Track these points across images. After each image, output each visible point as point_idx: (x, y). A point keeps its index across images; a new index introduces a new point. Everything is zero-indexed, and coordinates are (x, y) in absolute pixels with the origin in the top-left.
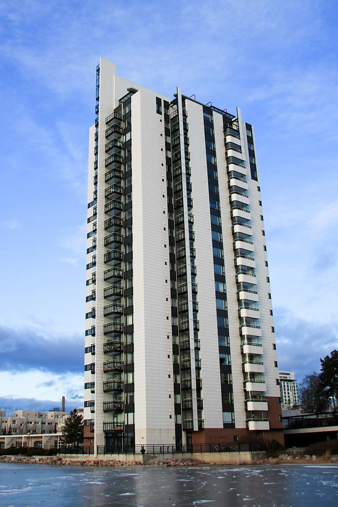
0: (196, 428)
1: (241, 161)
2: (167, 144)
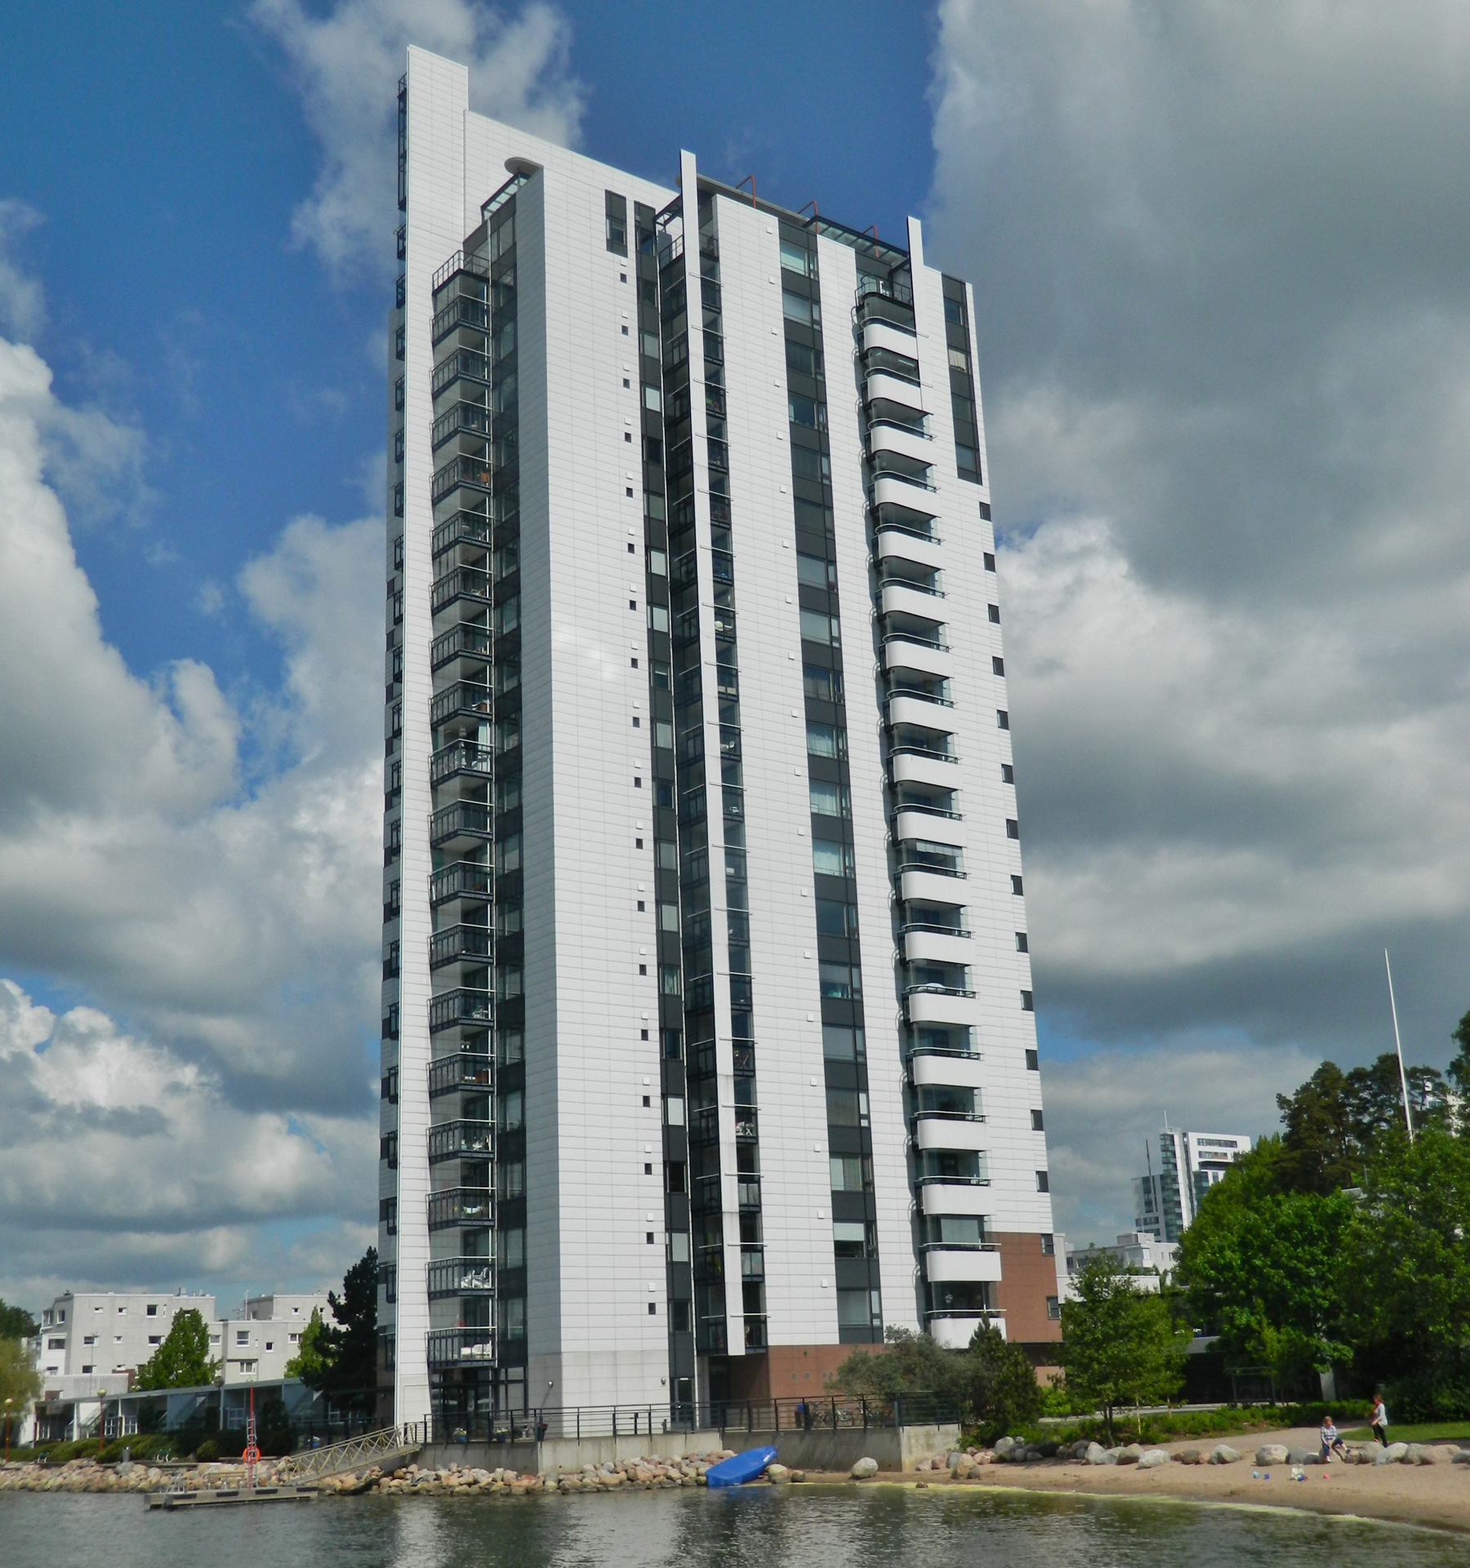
0: (736, 1345)
2: (643, 357)
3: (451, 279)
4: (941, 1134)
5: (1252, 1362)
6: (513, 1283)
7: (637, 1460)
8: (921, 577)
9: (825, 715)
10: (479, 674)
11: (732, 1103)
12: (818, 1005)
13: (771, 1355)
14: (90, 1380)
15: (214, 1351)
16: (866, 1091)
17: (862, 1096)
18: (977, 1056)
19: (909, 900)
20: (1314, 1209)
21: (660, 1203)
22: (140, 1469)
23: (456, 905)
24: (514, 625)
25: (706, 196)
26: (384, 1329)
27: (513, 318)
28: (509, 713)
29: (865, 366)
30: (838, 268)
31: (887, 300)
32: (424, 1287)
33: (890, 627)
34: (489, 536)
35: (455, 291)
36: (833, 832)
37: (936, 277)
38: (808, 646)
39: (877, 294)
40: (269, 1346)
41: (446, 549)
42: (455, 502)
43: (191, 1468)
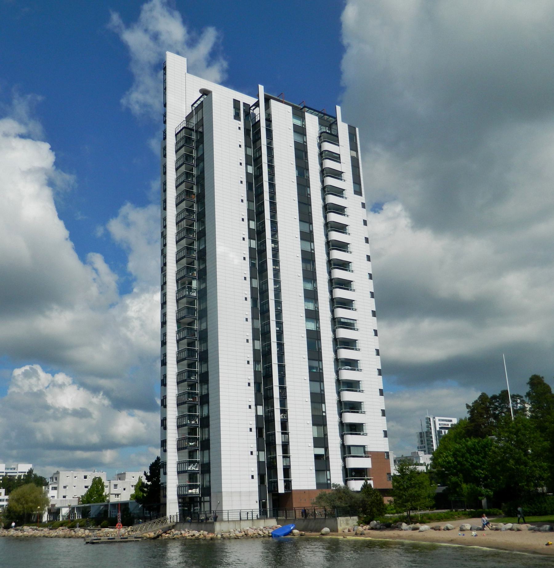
0: (281, 489)
3: (181, 130)
4: (350, 418)
6: (206, 468)
7: (248, 528)
9: (310, 275)
10: (192, 263)
11: (279, 407)
12: (308, 374)
13: (293, 493)
14: (66, 500)
15: (106, 491)
16: (325, 403)
17: (323, 405)
18: (362, 391)
21: (255, 441)
22: (82, 530)
23: (185, 341)
24: (203, 246)
25: (267, 100)
26: (162, 484)
27: (203, 143)
28: (202, 276)
29: (322, 157)
30: (312, 123)
31: (329, 134)
32: (176, 469)
34: (195, 216)
35: (183, 134)
36: (312, 315)
37: (346, 126)
38: (303, 252)
39: (326, 132)
41: (181, 221)
42: (183, 205)
43: (99, 530)
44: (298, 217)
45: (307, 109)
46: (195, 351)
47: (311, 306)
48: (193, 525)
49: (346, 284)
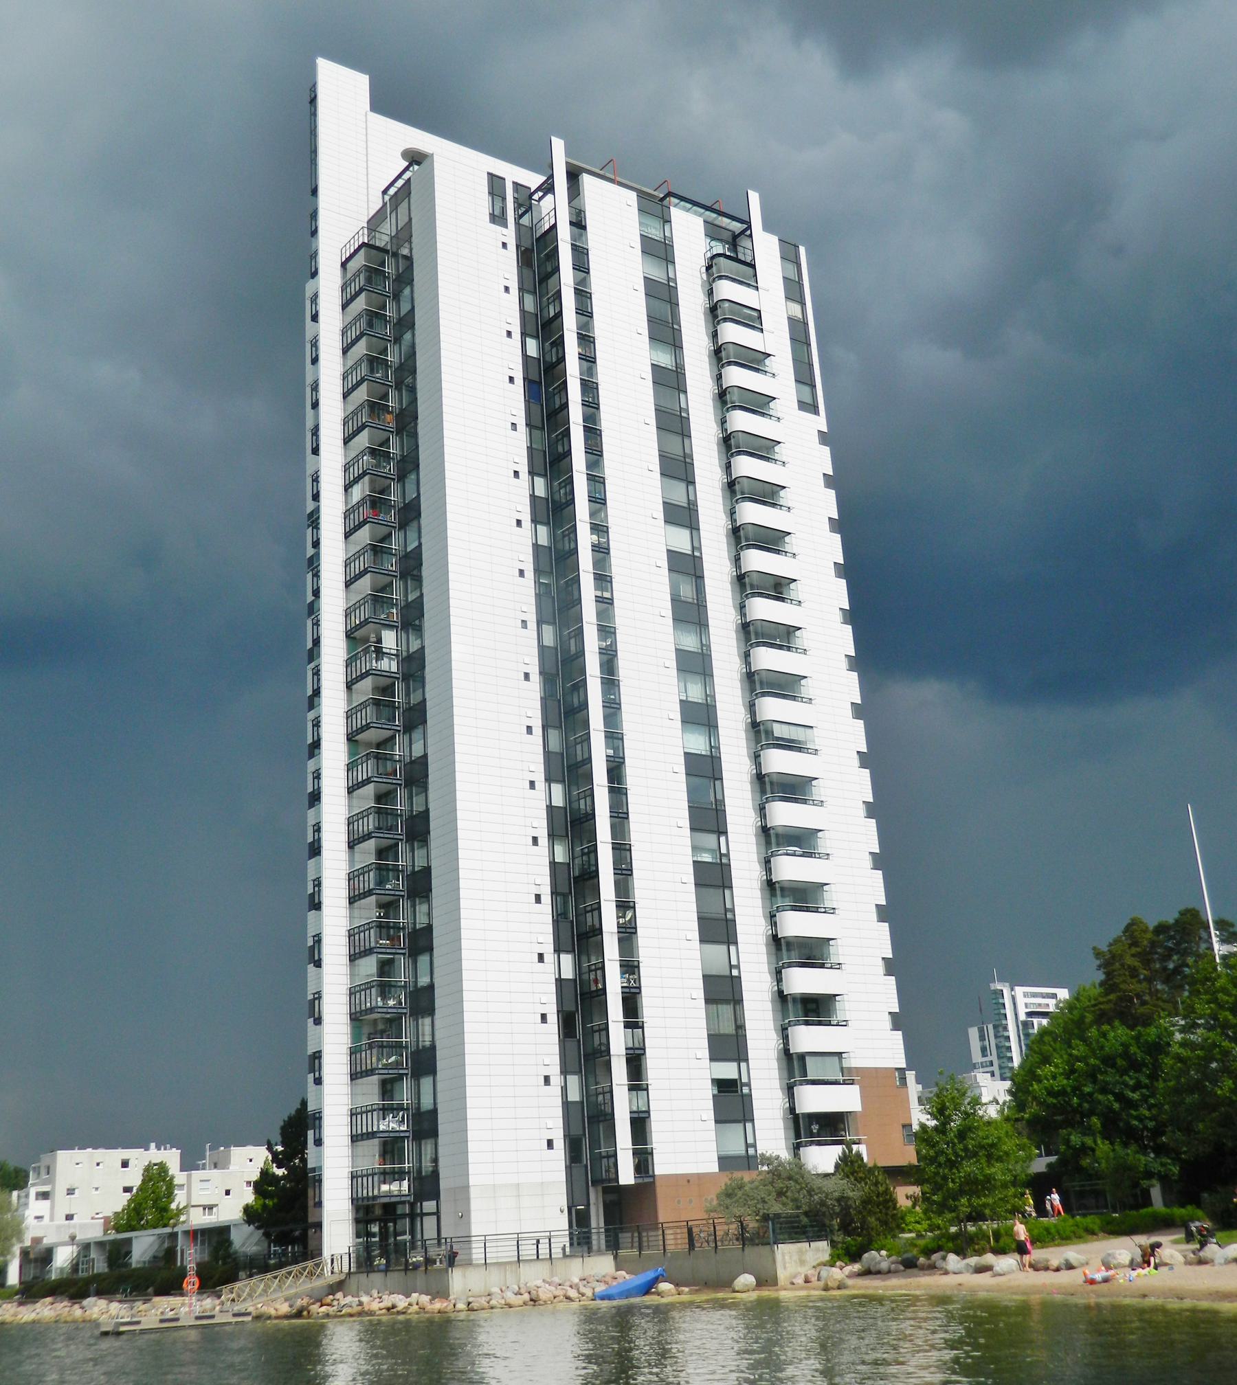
0: (627, 1176)
1: (762, 357)
2: (523, 311)
3: (356, 251)
4: (802, 981)
5: (1090, 1177)
6: (425, 1125)
7: (539, 1283)
8: (767, 494)
9: (690, 613)
13: (658, 1184)
19: (768, 775)
20: (1137, 1038)
21: (556, 1049)
22: (102, 1303)
23: (370, 790)
24: (416, 544)
25: (573, 176)
26: (314, 1170)
30: (689, 232)
33: (742, 537)
34: (391, 468)
35: (360, 261)
36: (700, 716)
37: (774, 240)
40: (228, 1193)
44: (657, 468)
45: (676, 201)
46: (394, 814)
47: (695, 693)
48: (395, 1277)
49: (782, 637)
